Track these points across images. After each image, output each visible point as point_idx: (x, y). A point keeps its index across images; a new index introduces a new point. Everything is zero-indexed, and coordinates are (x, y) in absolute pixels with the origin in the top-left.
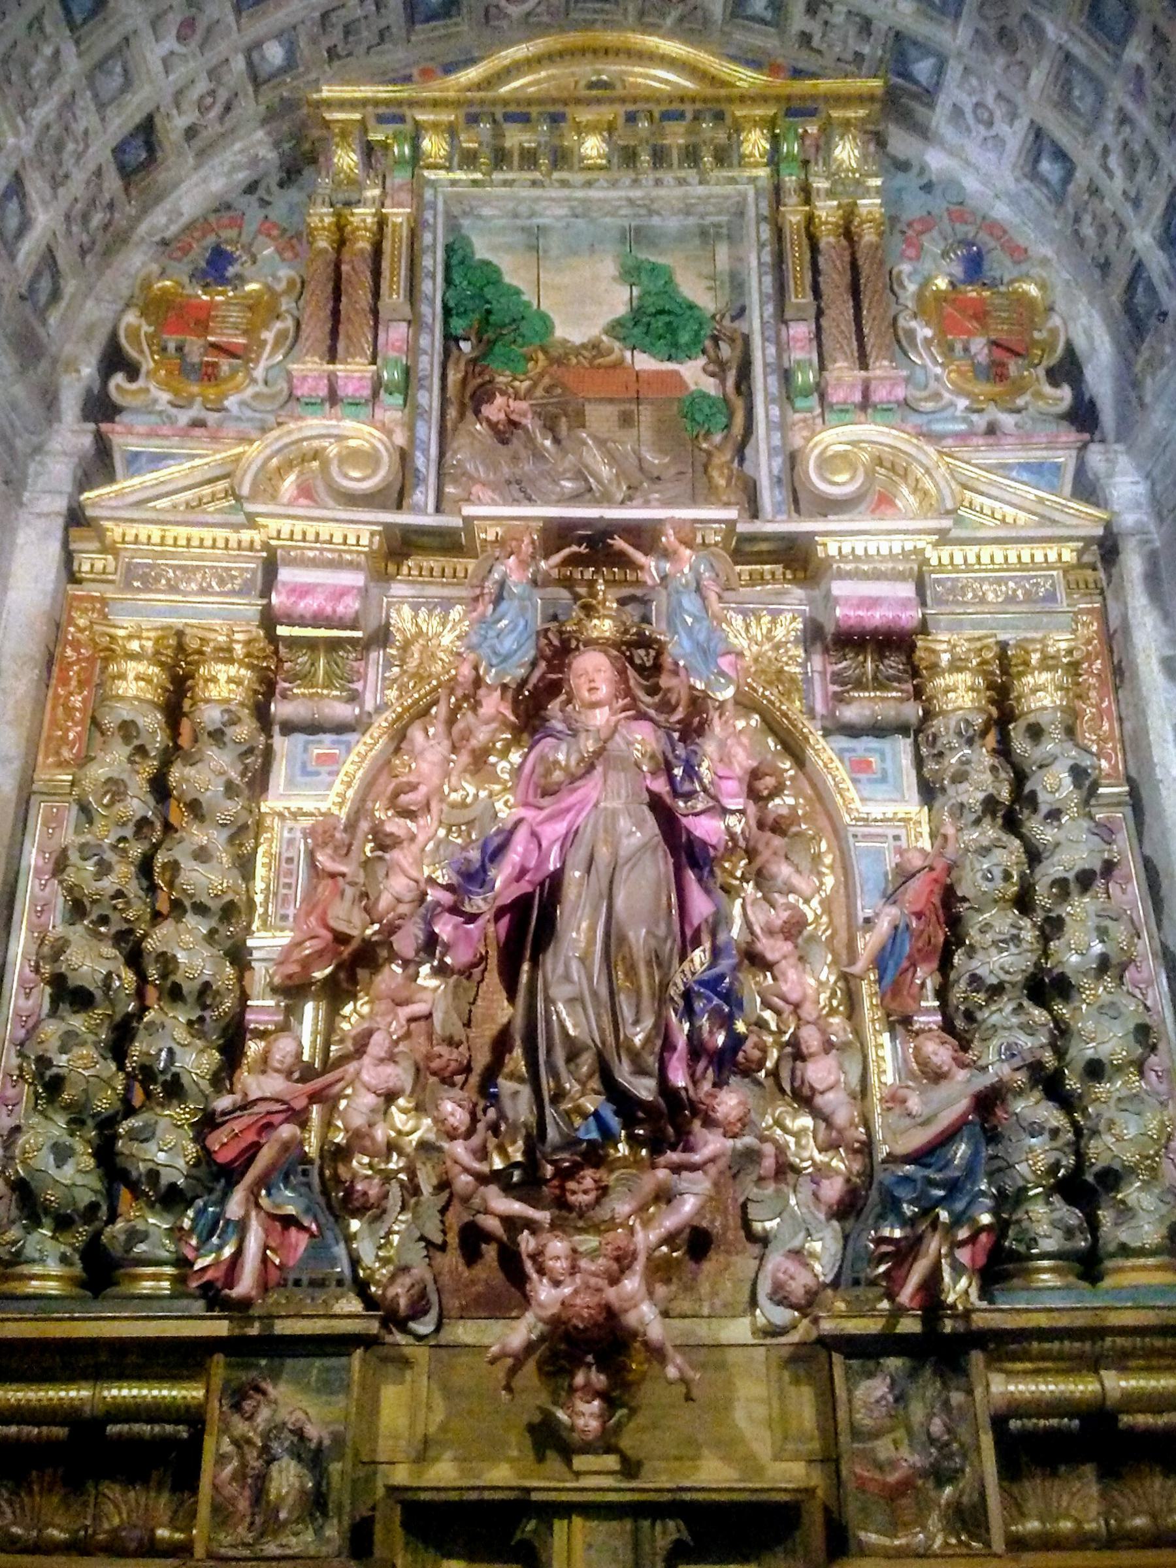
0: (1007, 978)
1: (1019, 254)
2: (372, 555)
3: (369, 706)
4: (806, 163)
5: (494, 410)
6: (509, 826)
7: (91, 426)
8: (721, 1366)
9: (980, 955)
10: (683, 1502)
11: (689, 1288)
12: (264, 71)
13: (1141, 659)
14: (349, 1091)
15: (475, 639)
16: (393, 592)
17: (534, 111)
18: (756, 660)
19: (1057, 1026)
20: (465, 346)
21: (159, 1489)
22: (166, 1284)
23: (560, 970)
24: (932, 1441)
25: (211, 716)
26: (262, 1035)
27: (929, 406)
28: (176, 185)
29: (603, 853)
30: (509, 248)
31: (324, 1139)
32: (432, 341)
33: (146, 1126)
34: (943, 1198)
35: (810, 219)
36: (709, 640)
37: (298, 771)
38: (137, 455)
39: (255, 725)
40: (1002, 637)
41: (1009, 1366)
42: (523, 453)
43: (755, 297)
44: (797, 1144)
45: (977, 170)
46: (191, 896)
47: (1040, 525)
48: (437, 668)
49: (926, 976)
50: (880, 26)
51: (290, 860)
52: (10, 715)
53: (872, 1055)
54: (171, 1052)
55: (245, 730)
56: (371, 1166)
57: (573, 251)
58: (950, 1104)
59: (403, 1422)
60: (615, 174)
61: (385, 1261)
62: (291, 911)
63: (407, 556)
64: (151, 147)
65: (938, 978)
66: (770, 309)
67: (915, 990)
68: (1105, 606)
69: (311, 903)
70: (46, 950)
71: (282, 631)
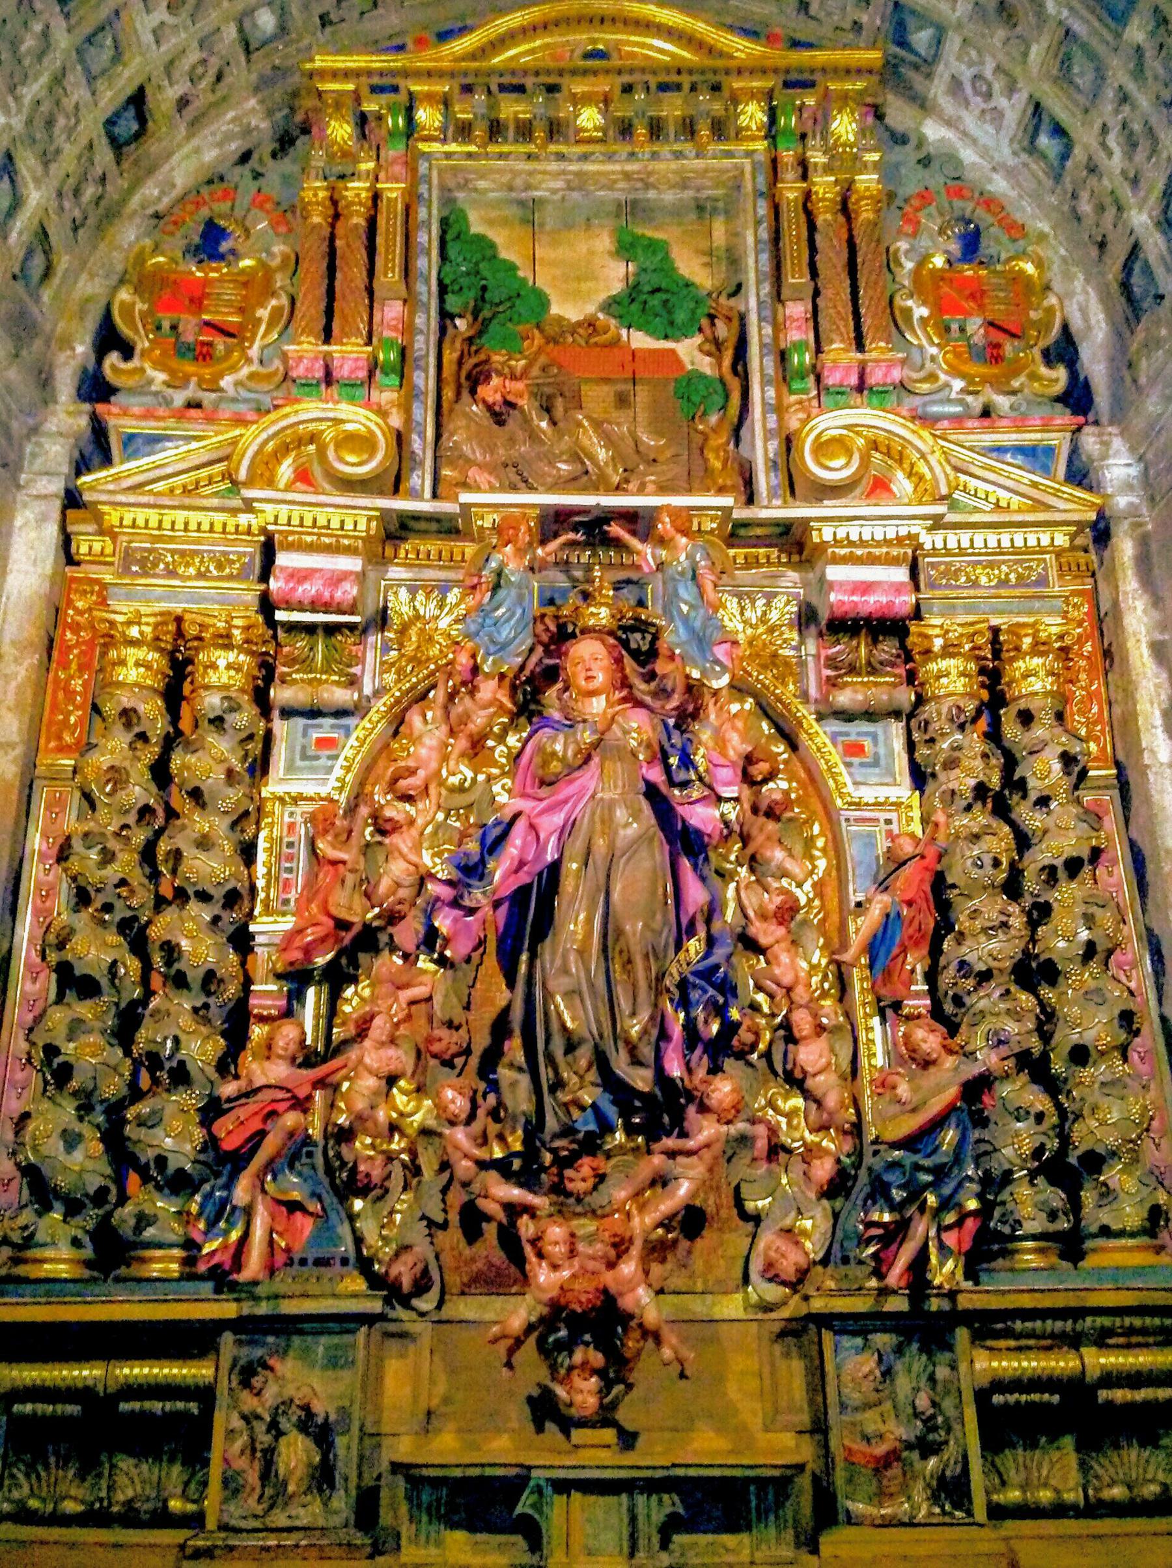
1: (1015, 230)
2: (367, 540)
3: (368, 690)
4: (803, 136)
5: (491, 391)
7: (87, 407)
8: (715, 1340)
9: (969, 942)
10: (678, 1478)
13: (1130, 644)
16: (390, 575)
17: (529, 82)
18: (750, 643)
19: (1043, 1011)
21: (172, 1461)
22: (175, 1266)
24: (916, 1415)
25: (212, 702)
26: (262, 1019)
27: (925, 387)
28: (169, 155)
29: (600, 843)
30: (505, 222)
32: (427, 320)
33: (153, 1112)
35: (808, 195)
36: (705, 627)
38: (132, 437)
39: (255, 710)
40: (995, 621)
42: (520, 435)
43: (752, 275)
44: (789, 1124)
45: (974, 141)
47: (1032, 509)
49: (916, 962)
51: (290, 845)
52: (11, 699)
53: (862, 1037)
54: (176, 1040)
55: (245, 717)
56: (373, 1146)
57: (569, 226)
58: (939, 1089)
62: (292, 896)
63: (404, 539)
64: (142, 119)
66: (766, 288)
67: (905, 976)
68: (1096, 588)
70: (52, 938)
71: (280, 616)
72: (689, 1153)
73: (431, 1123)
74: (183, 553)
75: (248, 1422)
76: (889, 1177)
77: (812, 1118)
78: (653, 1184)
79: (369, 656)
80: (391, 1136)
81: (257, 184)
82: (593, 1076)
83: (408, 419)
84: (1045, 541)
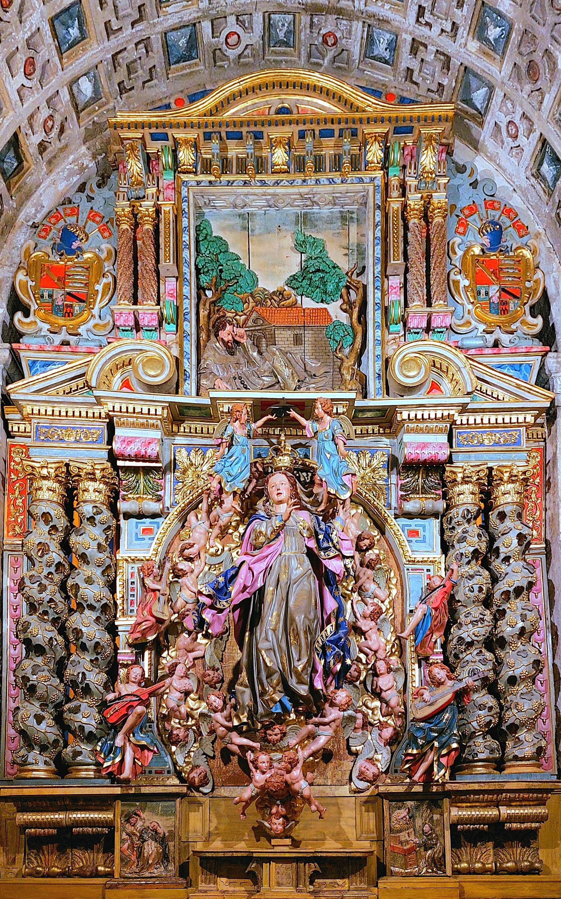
0: (476, 638)
3: (168, 504)
4: (404, 167)
5: (225, 334)
6: (238, 565)
7: (7, 345)
9: (464, 628)
11: (322, 774)
12: (82, 100)
14: (168, 691)
15: (219, 467)
17: (244, 130)
19: (497, 661)
20: (209, 293)
21: (98, 852)
22: (92, 773)
23: (263, 635)
25: (87, 509)
26: (126, 666)
27: (463, 329)
28: (38, 186)
30: (232, 229)
31: (158, 712)
32: (190, 290)
34: (436, 737)
35: (405, 206)
37: (134, 539)
41: (458, 805)
42: (242, 361)
44: (373, 713)
45: (504, 171)
46: (86, 601)
47: (516, 401)
48: (201, 483)
49: (438, 638)
50: (455, 62)
51: (133, 583)
56: (180, 723)
59: (199, 826)
60: (291, 177)
61: (188, 763)
63: (183, 422)
64: (19, 158)
65: (443, 638)
69: (143, 604)
71: (120, 463)
72: (325, 724)
73: (206, 711)
74: (66, 429)
75: (130, 836)
76: (418, 734)
77: (383, 710)
78: (308, 738)
79: (168, 486)
80: (188, 719)
81: (90, 205)
82: (280, 688)
83: (182, 351)
84: (521, 420)
